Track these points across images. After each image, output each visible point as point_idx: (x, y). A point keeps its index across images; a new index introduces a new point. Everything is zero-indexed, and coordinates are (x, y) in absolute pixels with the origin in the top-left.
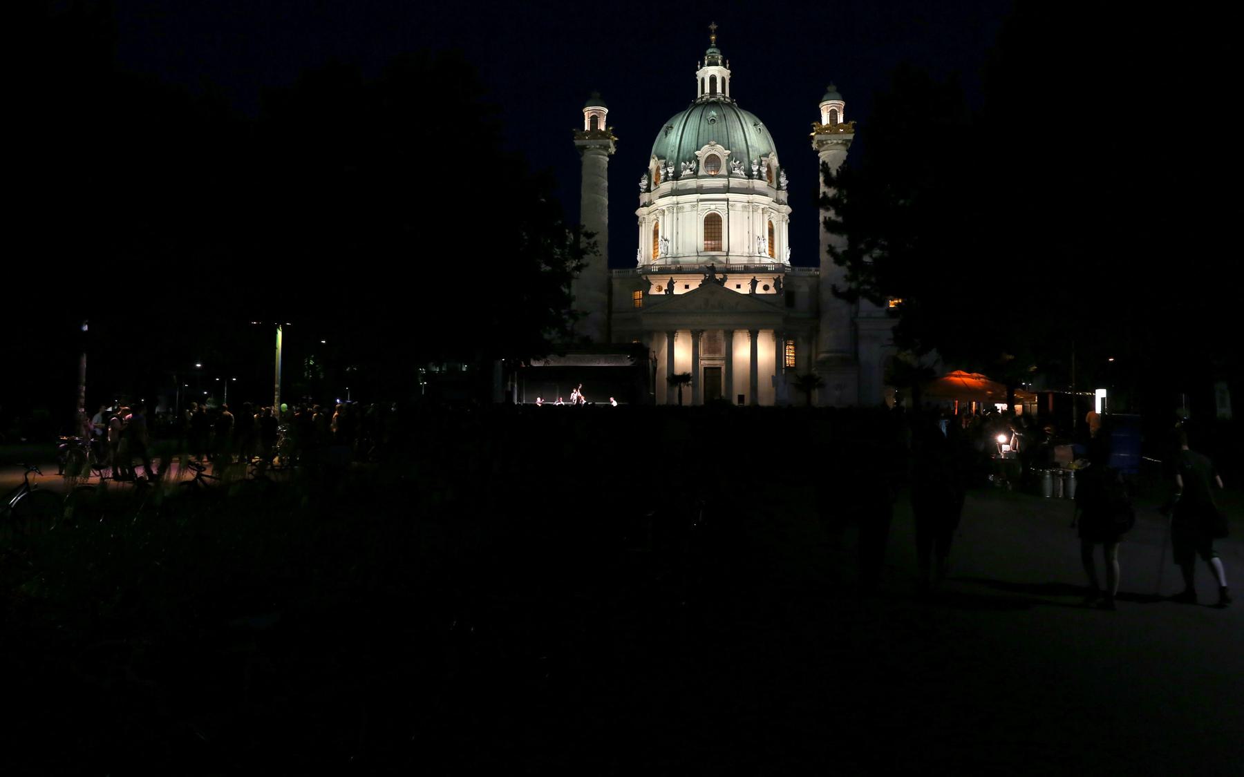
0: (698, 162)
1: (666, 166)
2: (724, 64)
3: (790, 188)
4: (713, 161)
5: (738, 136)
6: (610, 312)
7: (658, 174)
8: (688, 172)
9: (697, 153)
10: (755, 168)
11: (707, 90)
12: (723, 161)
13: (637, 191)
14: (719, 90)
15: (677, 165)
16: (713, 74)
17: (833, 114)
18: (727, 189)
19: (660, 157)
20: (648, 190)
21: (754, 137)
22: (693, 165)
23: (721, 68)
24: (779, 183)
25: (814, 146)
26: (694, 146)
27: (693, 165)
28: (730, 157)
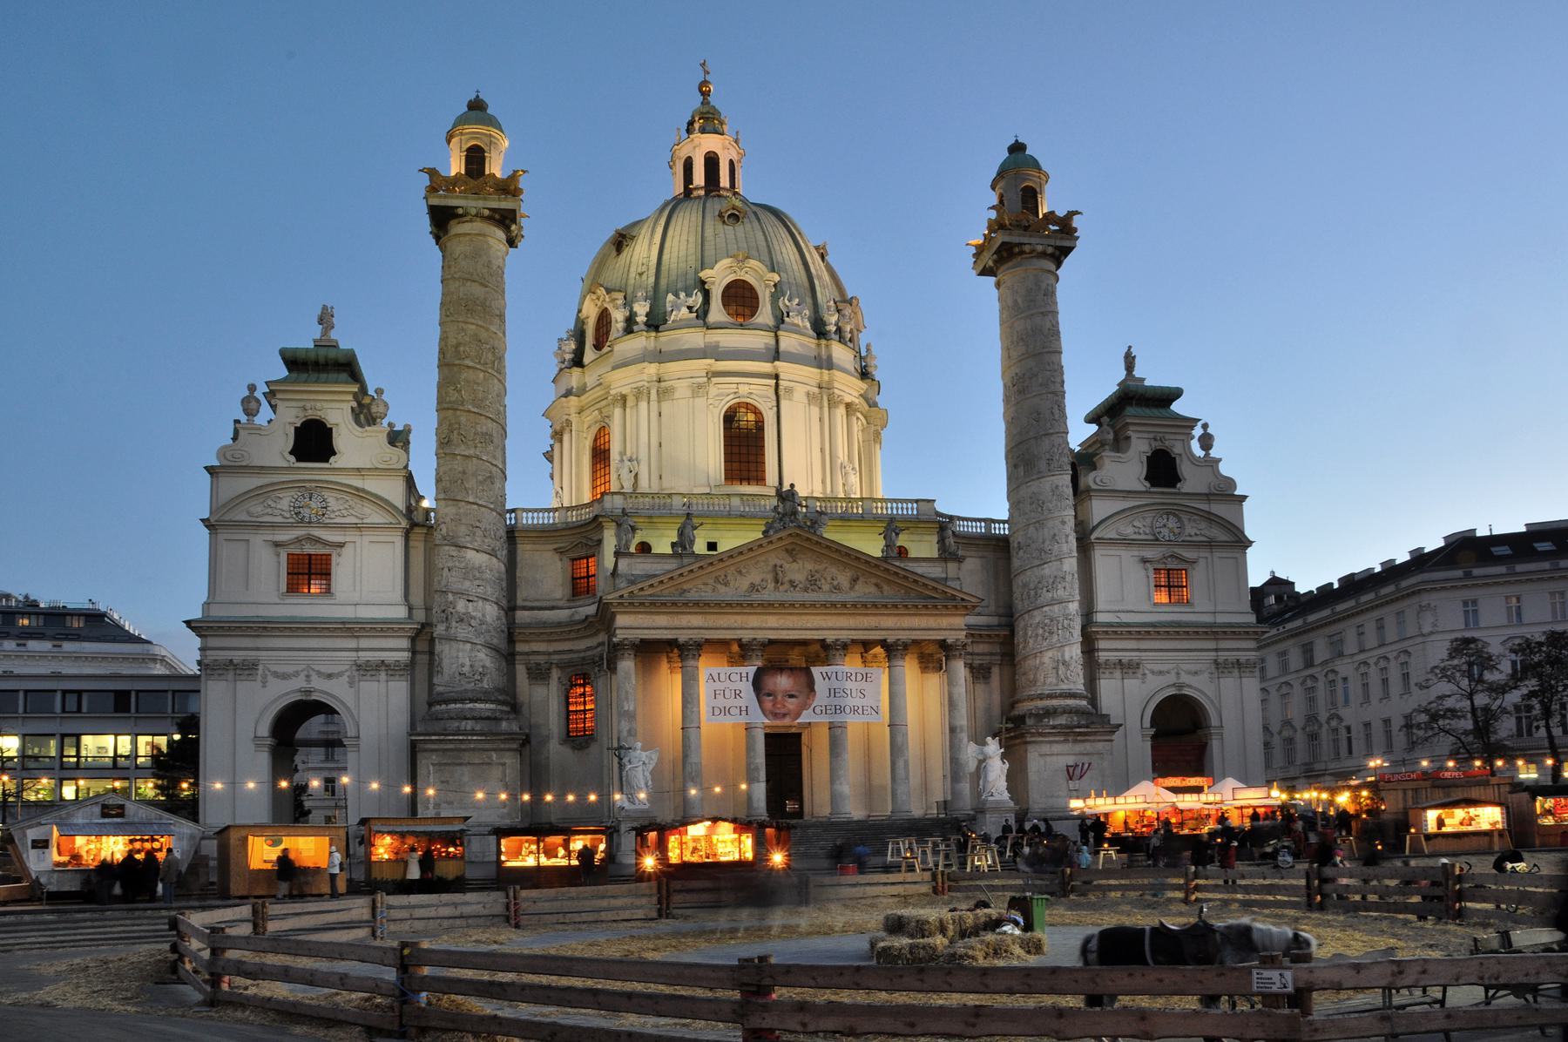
0: (707, 295)
1: (628, 303)
7: (604, 319)
15: (656, 297)
18: (776, 355)
22: (696, 300)
26: (693, 261)
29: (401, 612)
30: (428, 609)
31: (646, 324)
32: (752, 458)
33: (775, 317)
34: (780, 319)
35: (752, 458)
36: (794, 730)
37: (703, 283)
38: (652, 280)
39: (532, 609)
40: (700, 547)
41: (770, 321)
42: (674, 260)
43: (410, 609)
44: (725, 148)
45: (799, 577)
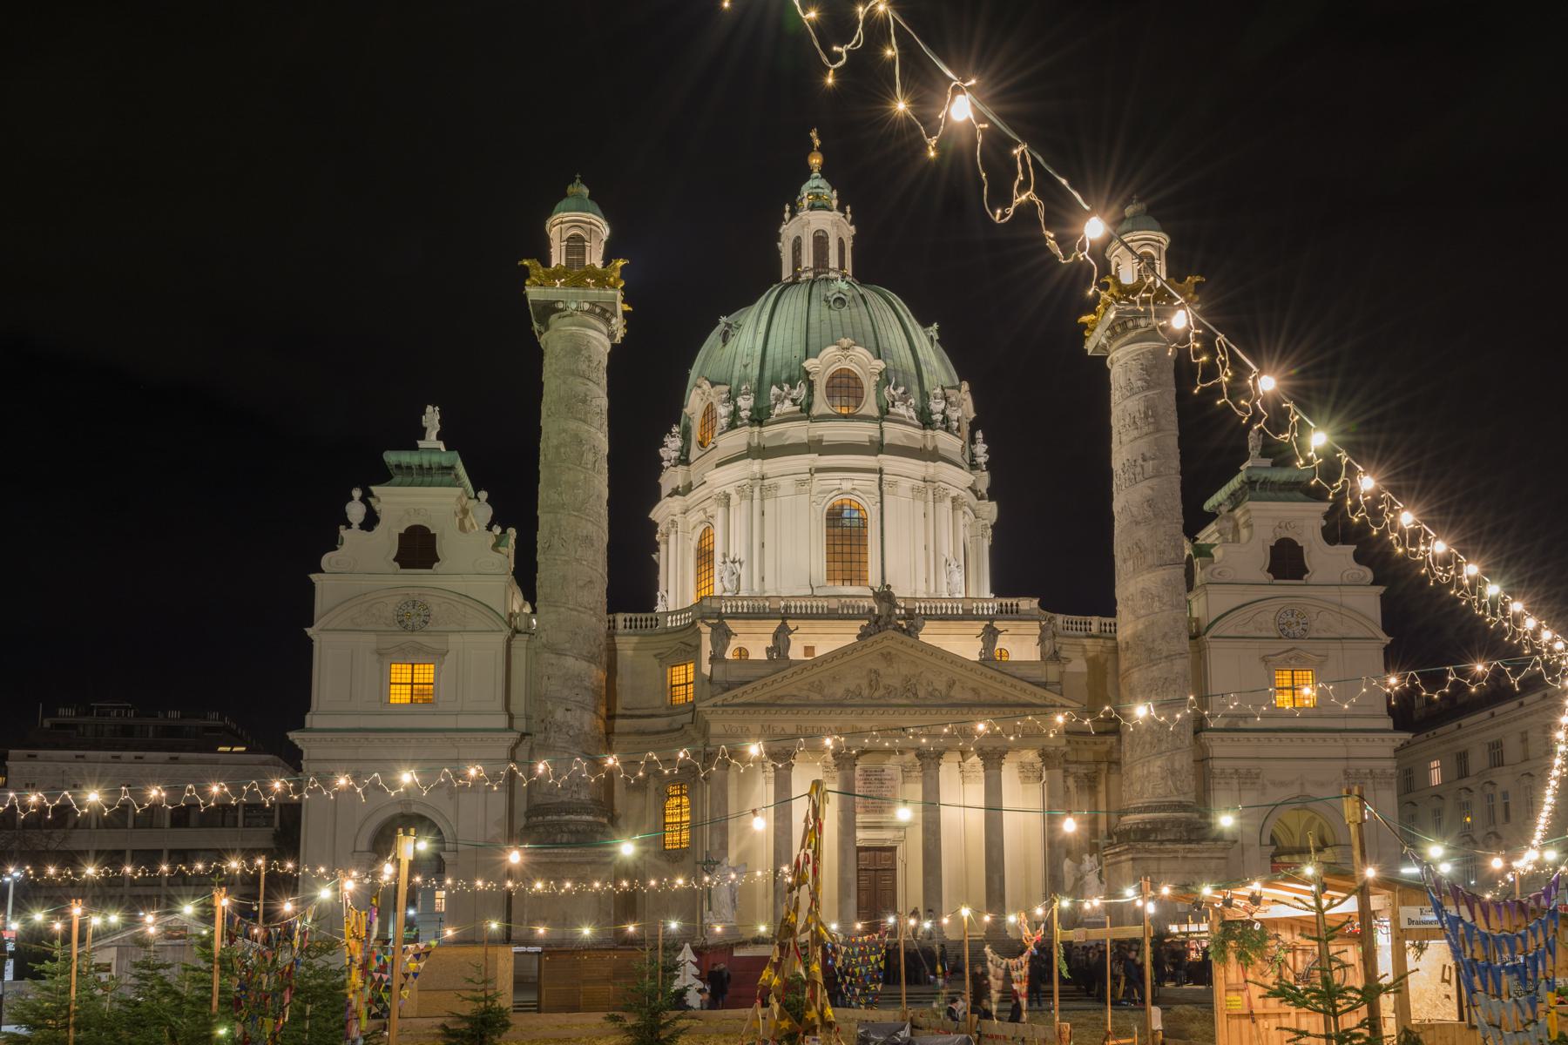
0: (811, 386)
1: (732, 397)
2: (841, 208)
4: (845, 386)
6: (611, 717)
7: (709, 412)
8: (787, 406)
9: (809, 364)
10: (937, 406)
11: (808, 260)
13: (657, 467)
14: (833, 262)
15: (760, 391)
18: (878, 447)
20: (684, 460)
22: (800, 392)
23: (838, 215)
26: (799, 351)
27: (800, 392)
28: (885, 379)
29: (502, 722)
30: (528, 718)
31: (750, 419)
32: (855, 557)
33: (880, 408)
34: (884, 414)
35: (855, 557)
36: (888, 844)
37: (808, 373)
38: (756, 372)
39: (632, 717)
40: (796, 653)
41: (876, 413)
42: (779, 350)
43: (511, 717)
44: (835, 224)
45: (896, 683)
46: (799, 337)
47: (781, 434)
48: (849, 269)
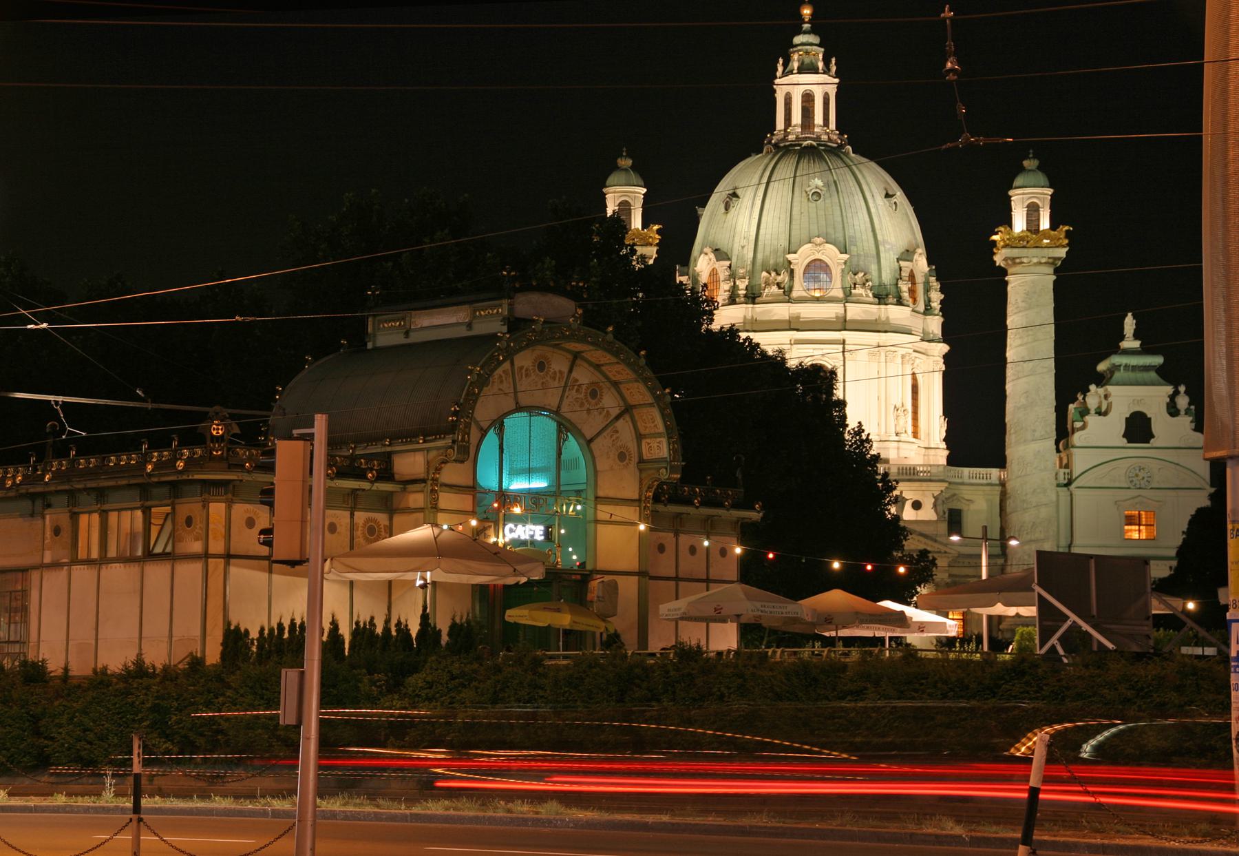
0: (792, 272)
1: (733, 276)
3: (945, 308)
4: (817, 268)
5: (859, 223)
9: (790, 257)
11: (797, 118)
12: (836, 271)
14: (818, 119)
16: (806, 89)
17: (1033, 210)
18: (844, 324)
19: (720, 254)
21: (883, 221)
22: (784, 277)
24: (928, 303)
25: (999, 259)
31: (745, 296)
34: (848, 297)
37: (790, 263)
38: (751, 255)
42: (768, 237)
46: (784, 227)
47: (769, 311)
48: (833, 125)
